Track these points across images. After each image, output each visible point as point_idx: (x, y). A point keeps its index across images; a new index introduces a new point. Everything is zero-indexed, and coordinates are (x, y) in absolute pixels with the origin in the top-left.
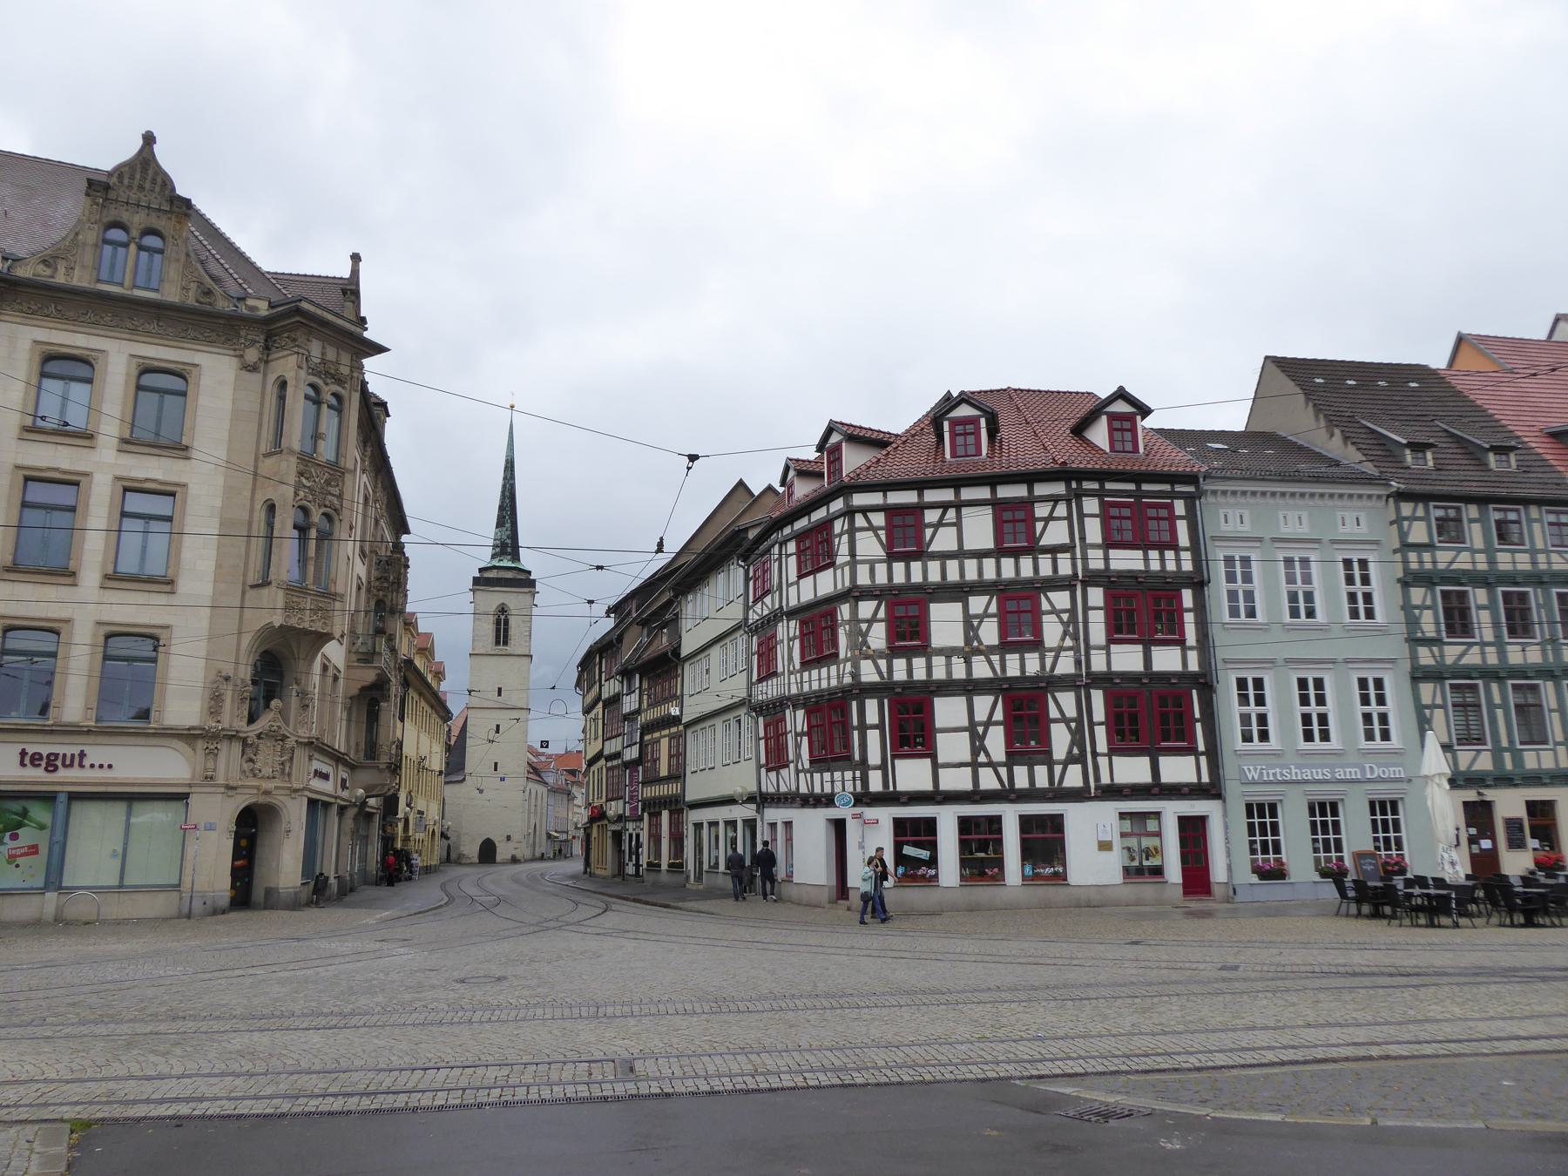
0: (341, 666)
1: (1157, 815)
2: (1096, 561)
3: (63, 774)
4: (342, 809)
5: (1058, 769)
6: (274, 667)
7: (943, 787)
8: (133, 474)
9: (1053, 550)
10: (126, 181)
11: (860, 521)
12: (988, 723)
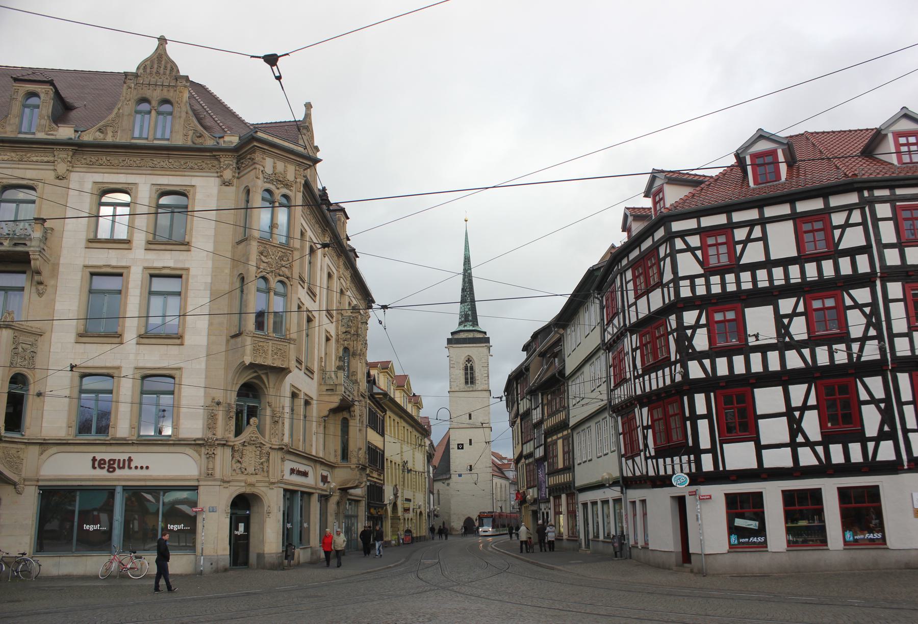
0: (313, 394)
2: (892, 258)
3: (119, 473)
4: (324, 498)
5: (871, 445)
7: (767, 464)
8: (156, 265)
9: (852, 253)
10: (148, 71)
11: (679, 244)
12: (805, 407)
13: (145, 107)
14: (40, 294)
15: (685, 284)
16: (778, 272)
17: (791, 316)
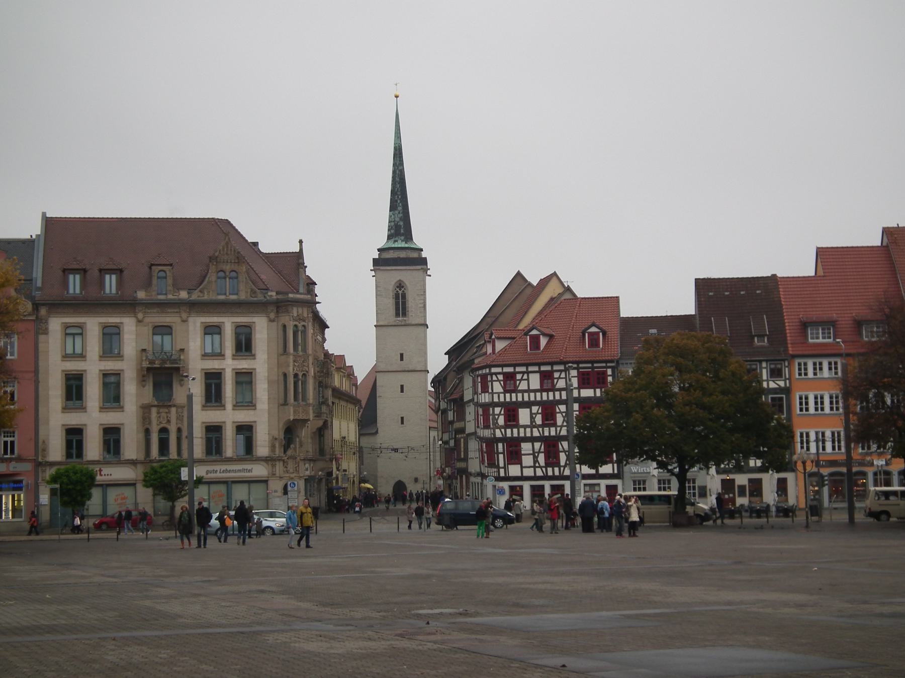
1: (599, 485)
2: (575, 394)
6: (290, 431)
8: (239, 367)
9: (560, 390)
11: (494, 378)
12: (539, 452)
13: (221, 274)
14: (181, 385)
15: (496, 396)
16: (532, 395)
17: (536, 414)
